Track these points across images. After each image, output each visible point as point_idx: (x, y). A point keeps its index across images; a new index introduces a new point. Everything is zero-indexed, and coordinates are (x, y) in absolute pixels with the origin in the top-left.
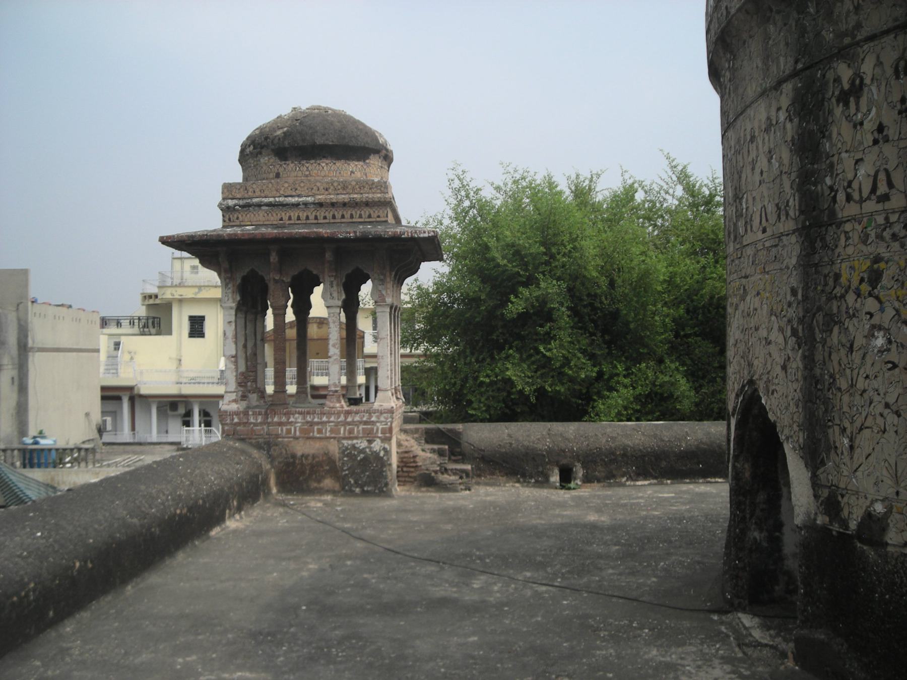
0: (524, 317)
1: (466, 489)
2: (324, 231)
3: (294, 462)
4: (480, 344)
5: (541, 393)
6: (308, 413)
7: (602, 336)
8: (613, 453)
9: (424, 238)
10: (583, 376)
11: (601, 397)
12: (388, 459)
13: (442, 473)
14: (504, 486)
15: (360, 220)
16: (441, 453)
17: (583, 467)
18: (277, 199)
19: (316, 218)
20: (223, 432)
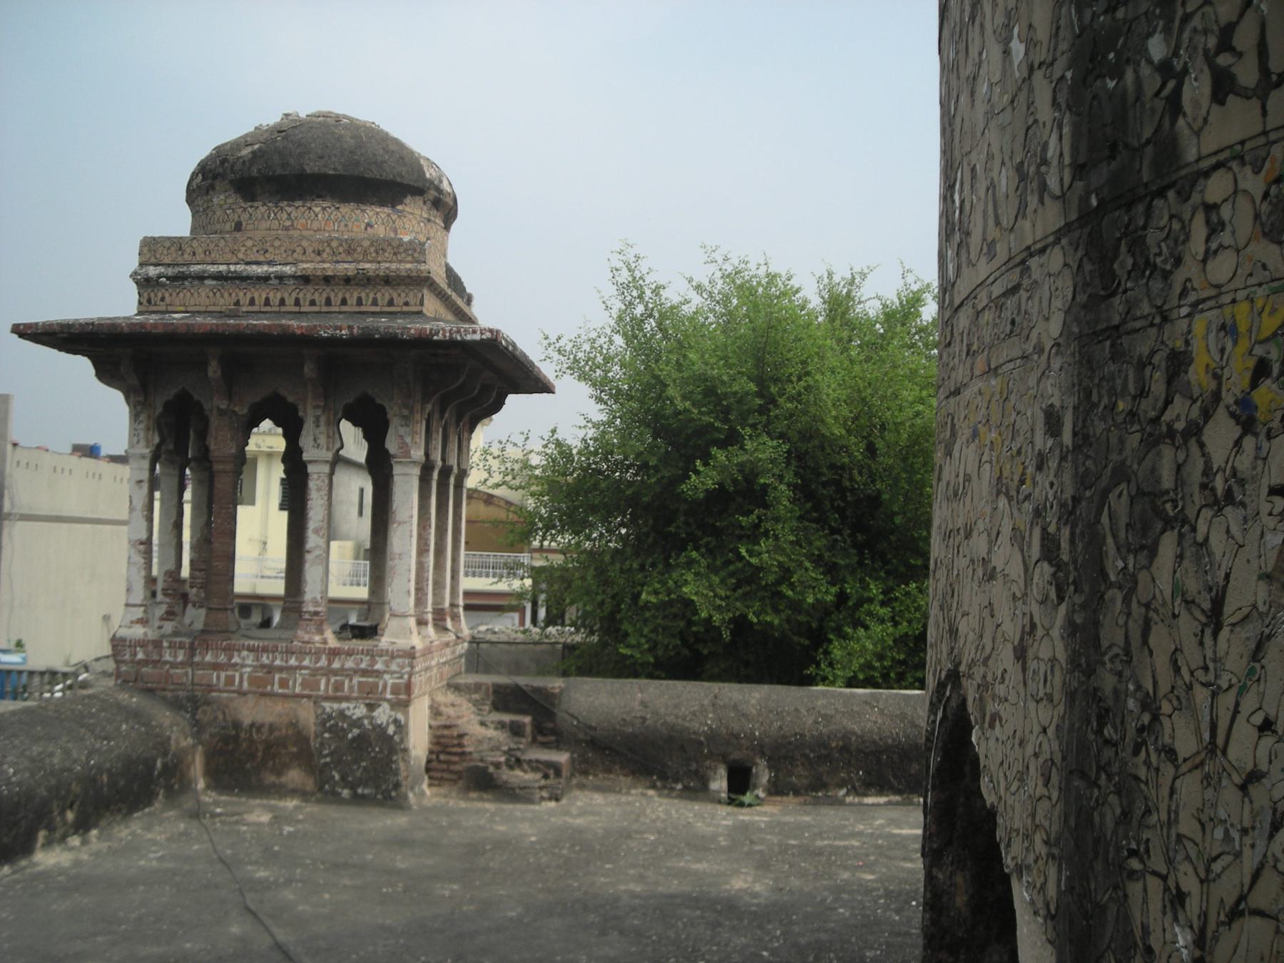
0: (720, 498)
1: (550, 799)
2: (297, 325)
3: (237, 737)
4: (650, 540)
5: (740, 624)
6: (265, 650)
7: (852, 535)
8: (825, 745)
9: (474, 342)
10: (810, 600)
11: (845, 637)
12: (402, 741)
13: (511, 768)
14: (628, 793)
15: (374, 309)
16: (516, 730)
17: (770, 768)
18: (232, 268)
19: (297, 303)
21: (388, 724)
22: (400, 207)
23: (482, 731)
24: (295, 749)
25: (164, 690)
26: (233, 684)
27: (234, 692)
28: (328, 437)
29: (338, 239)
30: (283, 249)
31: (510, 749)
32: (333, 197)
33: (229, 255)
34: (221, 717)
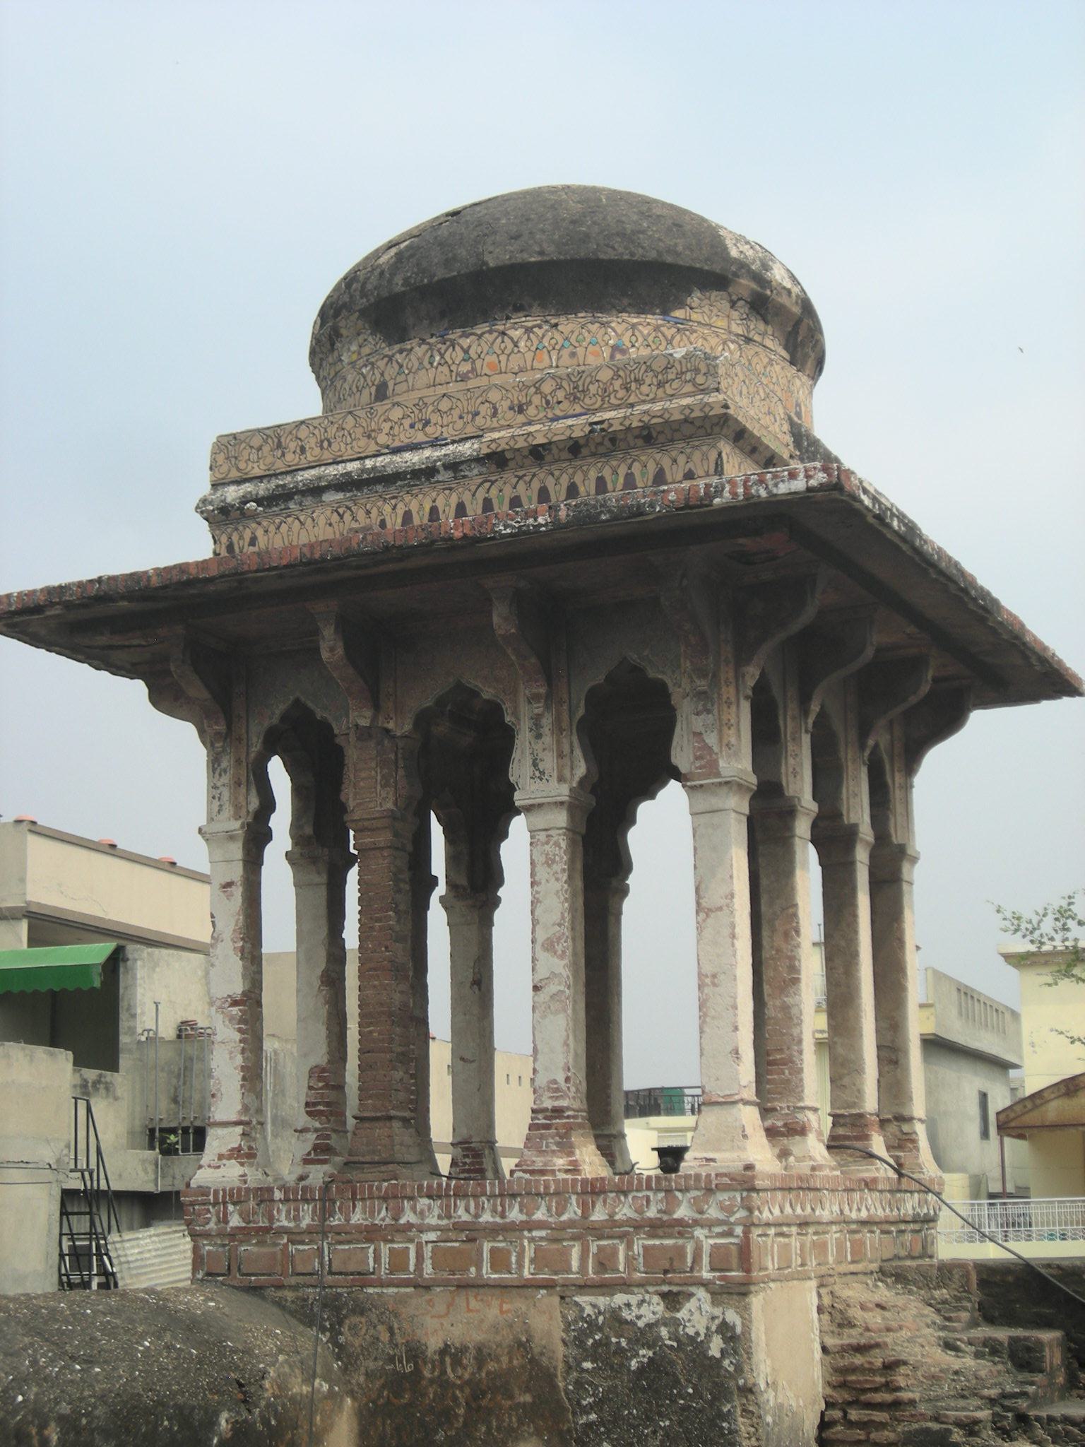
3: (417, 1372)
12: (739, 1369)
16: (1023, 1359)
18: (369, 463)
20: (198, 1260)
21: (708, 1335)
22: (679, 314)
23: (934, 1354)
24: (527, 1398)
25: (280, 1287)
26: (405, 1269)
27: (406, 1283)
28: (560, 755)
29: (553, 377)
30: (456, 413)
31: (1004, 1396)
32: (543, 306)
34: (385, 1336)
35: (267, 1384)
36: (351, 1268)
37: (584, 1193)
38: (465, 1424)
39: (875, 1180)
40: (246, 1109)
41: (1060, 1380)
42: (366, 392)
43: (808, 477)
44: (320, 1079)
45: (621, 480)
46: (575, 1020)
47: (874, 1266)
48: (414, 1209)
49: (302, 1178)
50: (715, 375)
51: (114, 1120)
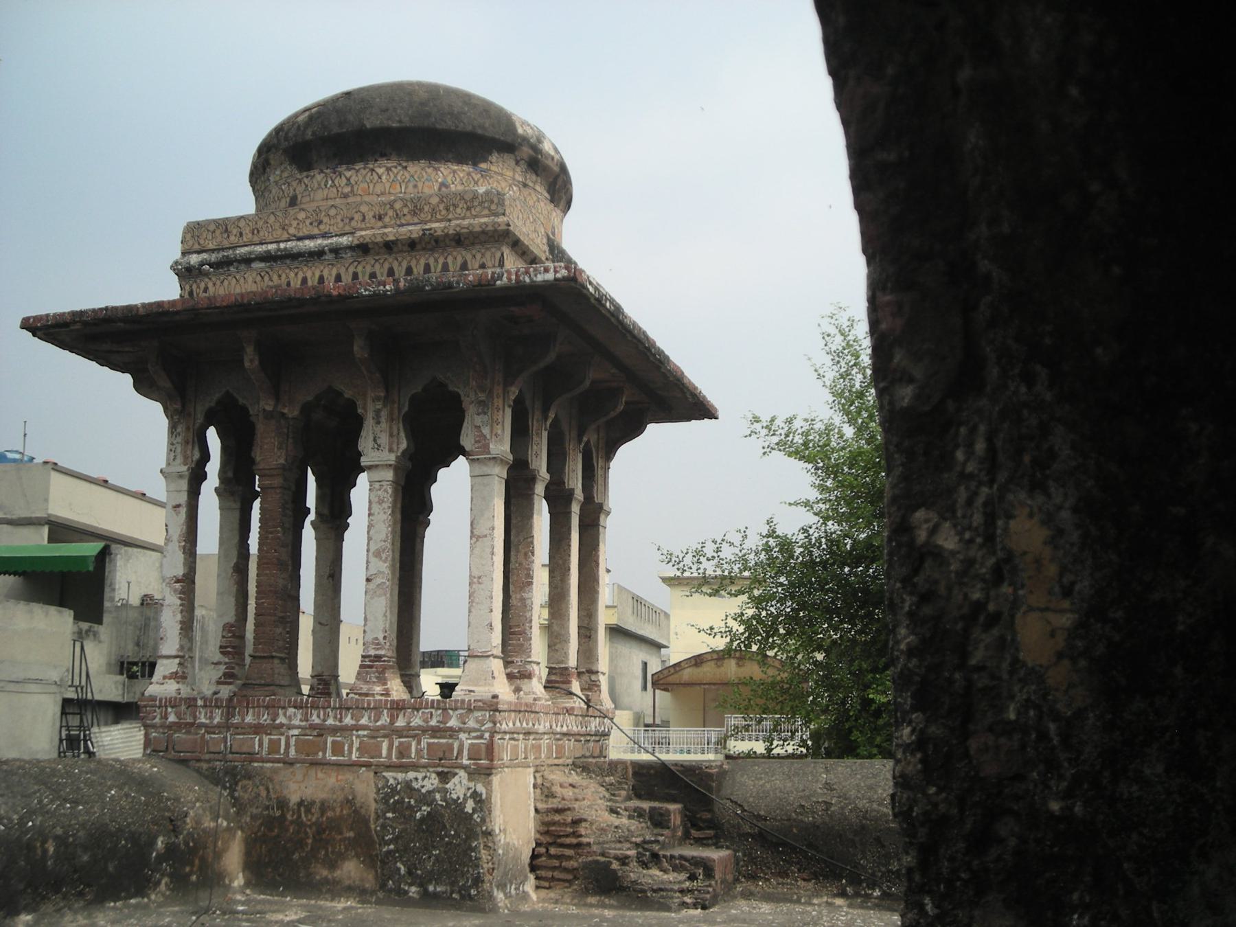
1: (695, 906)
3: (283, 816)
12: (483, 820)
13: (645, 865)
16: (658, 820)
18: (282, 246)
20: (147, 742)
21: (465, 799)
22: (483, 166)
23: (604, 817)
24: (351, 834)
25: (199, 760)
26: (278, 752)
27: (278, 761)
28: (391, 435)
31: (645, 842)
32: (399, 155)
33: (279, 232)
34: (264, 794)
35: (188, 820)
36: (245, 749)
37: (392, 708)
38: (312, 849)
39: (573, 708)
40: (182, 648)
41: (680, 834)
42: (283, 201)
43: (556, 272)
44: (230, 631)
45: (440, 266)
46: (392, 601)
47: (570, 761)
48: (285, 714)
49: (215, 693)
50: (503, 205)
51: (97, 656)
